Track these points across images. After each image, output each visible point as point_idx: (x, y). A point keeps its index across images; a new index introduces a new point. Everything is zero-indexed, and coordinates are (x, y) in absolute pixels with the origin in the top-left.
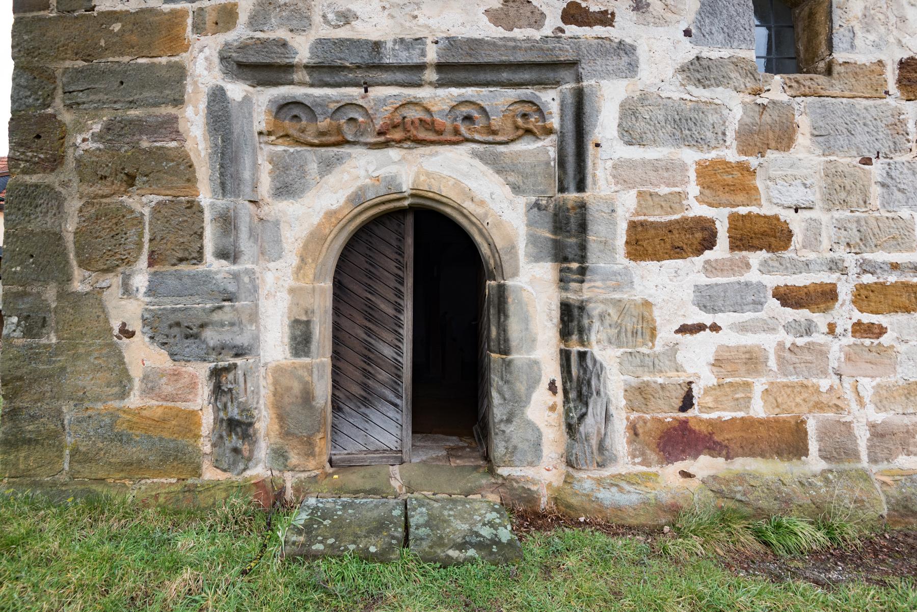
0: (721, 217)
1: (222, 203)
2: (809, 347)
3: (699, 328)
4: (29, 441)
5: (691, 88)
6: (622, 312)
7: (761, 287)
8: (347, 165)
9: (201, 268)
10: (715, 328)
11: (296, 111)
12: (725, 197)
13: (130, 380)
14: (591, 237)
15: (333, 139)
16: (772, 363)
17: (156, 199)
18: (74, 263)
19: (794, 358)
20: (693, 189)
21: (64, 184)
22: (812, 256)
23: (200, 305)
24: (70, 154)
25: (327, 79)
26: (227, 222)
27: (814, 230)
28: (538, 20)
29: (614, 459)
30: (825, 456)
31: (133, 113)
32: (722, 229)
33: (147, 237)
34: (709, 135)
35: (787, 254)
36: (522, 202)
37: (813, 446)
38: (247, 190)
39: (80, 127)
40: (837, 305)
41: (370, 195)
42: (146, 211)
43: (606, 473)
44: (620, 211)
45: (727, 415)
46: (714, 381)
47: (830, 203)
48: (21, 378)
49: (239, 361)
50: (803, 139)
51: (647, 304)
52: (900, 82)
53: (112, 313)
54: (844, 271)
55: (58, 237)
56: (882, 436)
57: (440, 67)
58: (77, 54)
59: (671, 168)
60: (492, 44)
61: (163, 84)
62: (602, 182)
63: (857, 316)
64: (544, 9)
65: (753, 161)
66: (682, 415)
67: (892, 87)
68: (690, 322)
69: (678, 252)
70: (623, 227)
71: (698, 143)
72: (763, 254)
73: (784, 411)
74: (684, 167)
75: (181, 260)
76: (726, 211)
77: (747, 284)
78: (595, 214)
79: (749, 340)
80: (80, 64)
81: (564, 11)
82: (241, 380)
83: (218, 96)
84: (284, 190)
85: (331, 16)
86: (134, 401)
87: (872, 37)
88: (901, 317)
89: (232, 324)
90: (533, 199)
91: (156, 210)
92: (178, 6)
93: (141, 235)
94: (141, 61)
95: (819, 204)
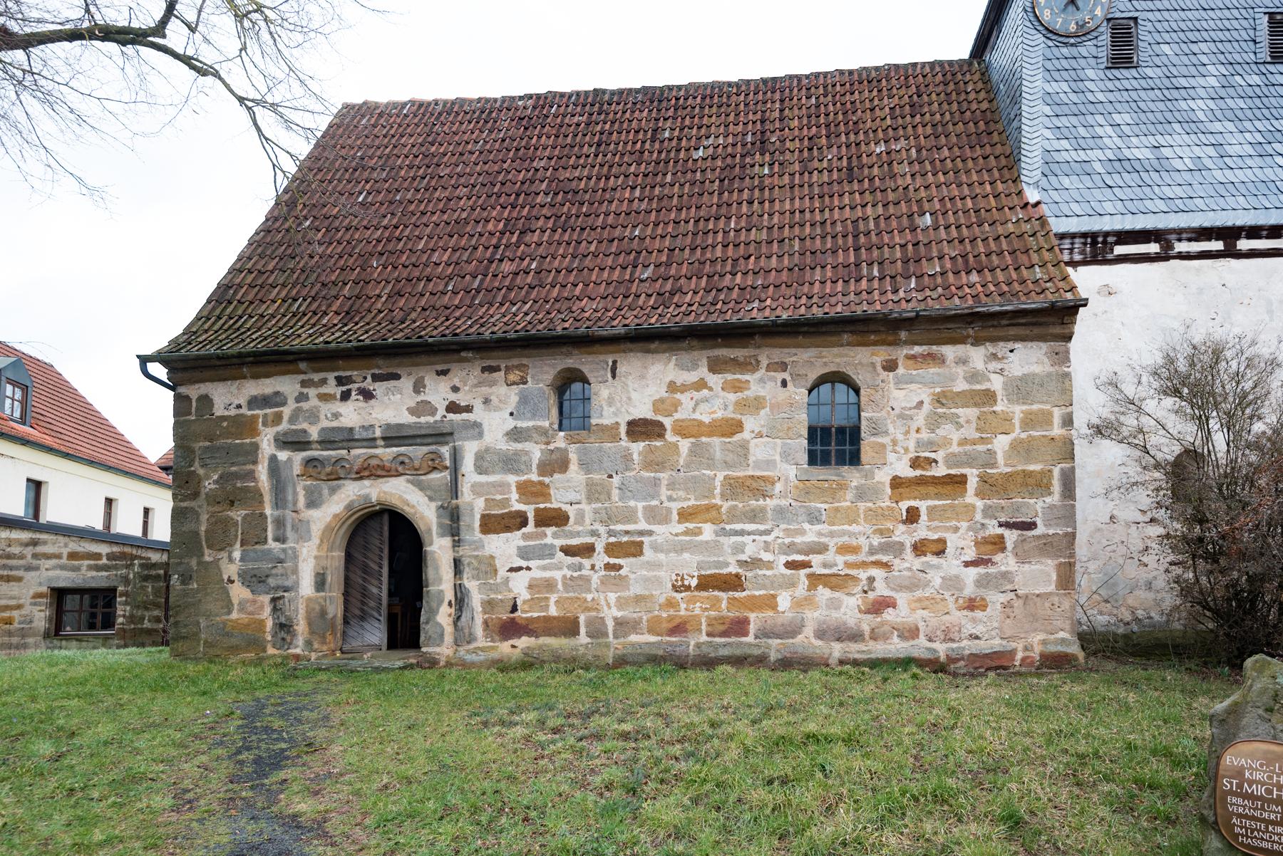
0: (530, 510)
1: (276, 513)
2: (580, 577)
3: (520, 569)
4: (184, 638)
5: (511, 443)
6: (480, 562)
7: (553, 546)
8: (343, 490)
9: (266, 547)
10: (528, 569)
11: (316, 463)
12: (533, 499)
13: (233, 605)
14: (462, 523)
15: (333, 477)
16: (560, 586)
17: (244, 512)
18: (205, 546)
19: (573, 584)
20: (514, 496)
21: (199, 507)
22: (581, 528)
23: (266, 566)
24: (203, 491)
25: (329, 446)
26: (279, 523)
27: (581, 517)
28: (433, 411)
29: (475, 639)
30: (589, 635)
31: (234, 469)
32: (531, 516)
33: (240, 532)
34: (523, 467)
35: (567, 528)
36: (434, 505)
37: (583, 630)
38: (290, 505)
39: (208, 477)
40: (595, 554)
41: (356, 505)
42: (239, 519)
43: (472, 646)
44: (476, 509)
45: (535, 615)
46: (529, 597)
47: (590, 500)
48: (179, 606)
49: (286, 594)
50: (573, 467)
51: (492, 557)
52: (628, 433)
53: (224, 571)
54: (599, 536)
55: (197, 534)
56: (621, 624)
57: (384, 438)
58: (205, 439)
59: (503, 486)
60: (409, 426)
61: (247, 453)
62: (466, 495)
63: (607, 559)
64: (437, 406)
65: (547, 480)
66: (512, 615)
67: (623, 435)
68: (514, 566)
69: (508, 529)
70: (478, 517)
71: (516, 472)
72: (554, 529)
73: (568, 612)
74: (509, 485)
75: (256, 543)
76: (533, 507)
77: (545, 545)
78: (464, 511)
79: (547, 574)
80: (208, 444)
81: (447, 406)
82: (287, 604)
83: (273, 459)
84: (312, 503)
85: (329, 415)
86: (234, 615)
87: (612, 409)
88: (632, 560)
89: (282, 575)
90: (440, 503)
91: (244, 518)
92: (255, 412)
93: (237, 531)
94: (237, 441)
95: (584, 501)
